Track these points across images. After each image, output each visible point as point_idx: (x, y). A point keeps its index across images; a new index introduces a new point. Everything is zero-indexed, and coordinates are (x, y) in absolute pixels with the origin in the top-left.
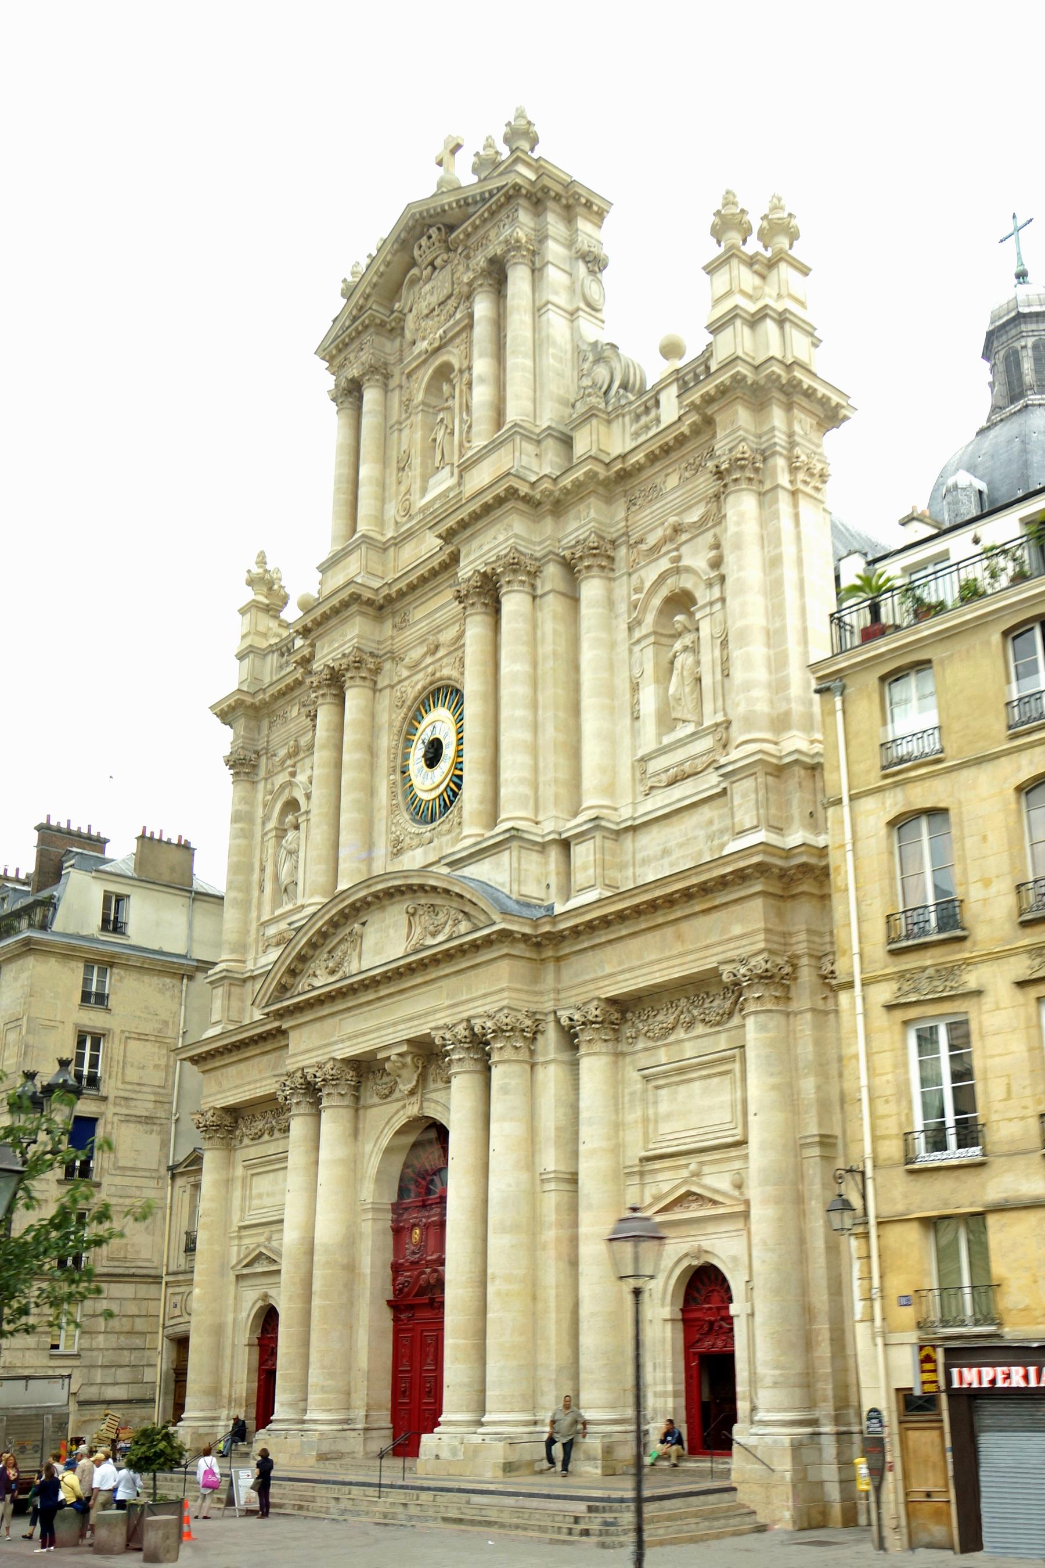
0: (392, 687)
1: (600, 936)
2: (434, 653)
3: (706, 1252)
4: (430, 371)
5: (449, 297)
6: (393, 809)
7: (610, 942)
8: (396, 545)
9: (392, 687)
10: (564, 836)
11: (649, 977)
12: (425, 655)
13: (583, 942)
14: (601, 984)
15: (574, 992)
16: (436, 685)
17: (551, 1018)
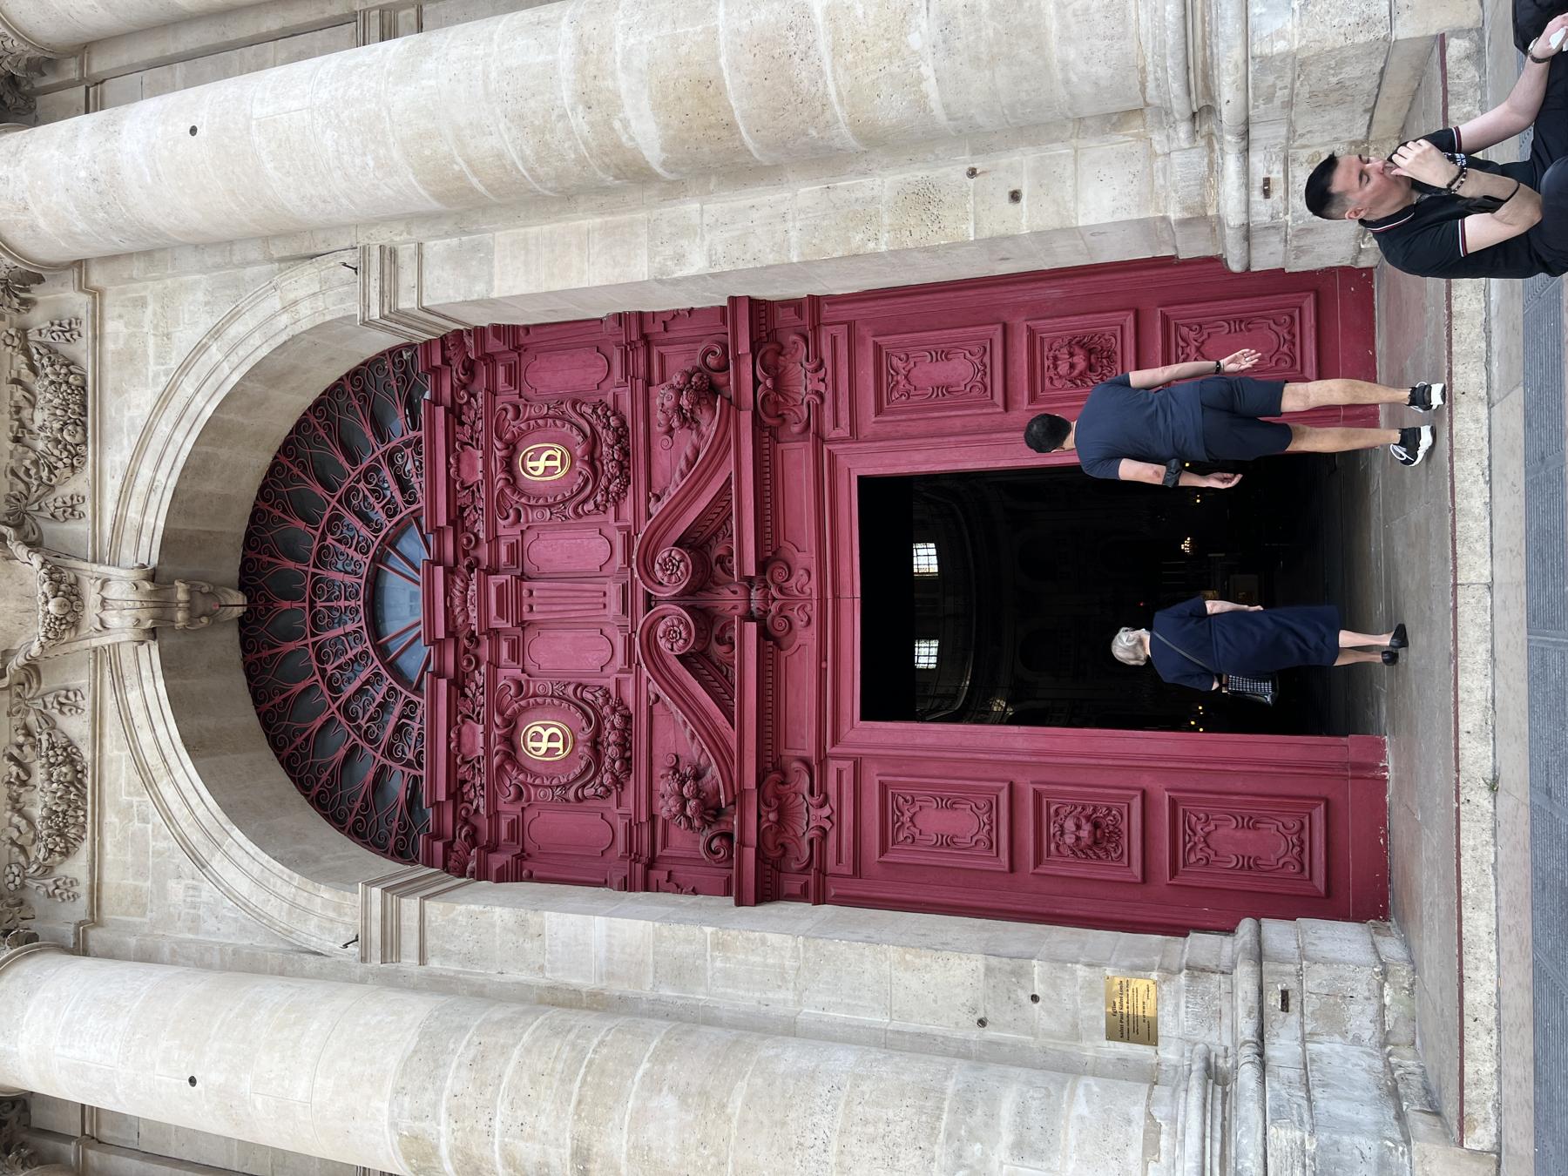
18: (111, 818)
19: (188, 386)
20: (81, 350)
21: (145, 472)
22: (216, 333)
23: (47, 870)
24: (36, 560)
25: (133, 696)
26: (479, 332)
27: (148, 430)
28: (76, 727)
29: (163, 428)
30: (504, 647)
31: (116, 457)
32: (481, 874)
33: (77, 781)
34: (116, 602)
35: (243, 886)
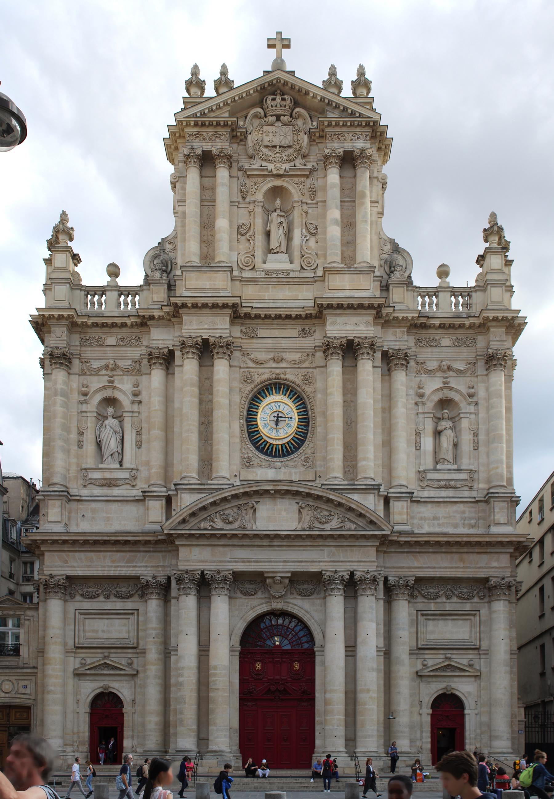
0: (240, 367)
1: (416, 548)
2: (278, 363)
3: (453, 689)
4: (270, 185)
5: (290, 147)
6: (242, 438)
7: (419, 552)
8: (241, 281)
9: (240, 367)
10: (389, 495)
11: (443, 573)
12: (269, 360)
13: (404, 548)
14: (413, 570)
15: (395, 570)
16: (278, 381)
17: (383, 579)
18: (247, 600)
19: (308, 616)
20: (315, 595)
21: (297, 608)
22: (315, 621)
23: (239, 589)
24: (284, 593)
25: (264, 605)
26: (315, 658)
27: (302, 609)
28: (259, 594)
29: (303, 611)
30: (270, 660)
31: (299, 602)
32: (240, 657)
33: (252, 595)
34: (278, 605)
35: (238, 626)
